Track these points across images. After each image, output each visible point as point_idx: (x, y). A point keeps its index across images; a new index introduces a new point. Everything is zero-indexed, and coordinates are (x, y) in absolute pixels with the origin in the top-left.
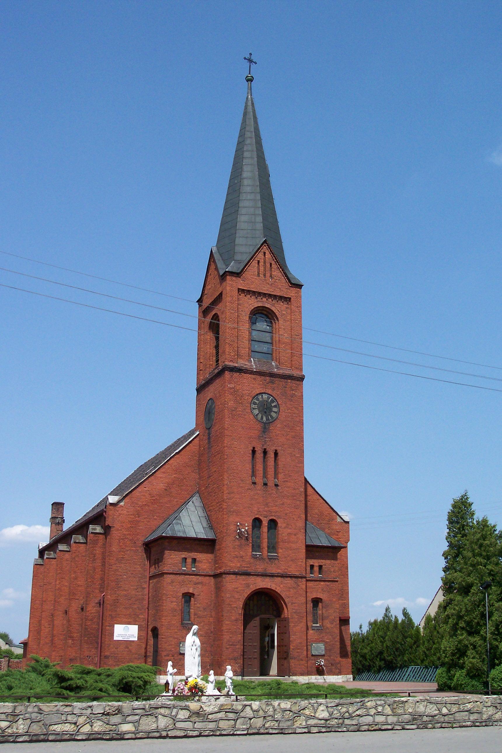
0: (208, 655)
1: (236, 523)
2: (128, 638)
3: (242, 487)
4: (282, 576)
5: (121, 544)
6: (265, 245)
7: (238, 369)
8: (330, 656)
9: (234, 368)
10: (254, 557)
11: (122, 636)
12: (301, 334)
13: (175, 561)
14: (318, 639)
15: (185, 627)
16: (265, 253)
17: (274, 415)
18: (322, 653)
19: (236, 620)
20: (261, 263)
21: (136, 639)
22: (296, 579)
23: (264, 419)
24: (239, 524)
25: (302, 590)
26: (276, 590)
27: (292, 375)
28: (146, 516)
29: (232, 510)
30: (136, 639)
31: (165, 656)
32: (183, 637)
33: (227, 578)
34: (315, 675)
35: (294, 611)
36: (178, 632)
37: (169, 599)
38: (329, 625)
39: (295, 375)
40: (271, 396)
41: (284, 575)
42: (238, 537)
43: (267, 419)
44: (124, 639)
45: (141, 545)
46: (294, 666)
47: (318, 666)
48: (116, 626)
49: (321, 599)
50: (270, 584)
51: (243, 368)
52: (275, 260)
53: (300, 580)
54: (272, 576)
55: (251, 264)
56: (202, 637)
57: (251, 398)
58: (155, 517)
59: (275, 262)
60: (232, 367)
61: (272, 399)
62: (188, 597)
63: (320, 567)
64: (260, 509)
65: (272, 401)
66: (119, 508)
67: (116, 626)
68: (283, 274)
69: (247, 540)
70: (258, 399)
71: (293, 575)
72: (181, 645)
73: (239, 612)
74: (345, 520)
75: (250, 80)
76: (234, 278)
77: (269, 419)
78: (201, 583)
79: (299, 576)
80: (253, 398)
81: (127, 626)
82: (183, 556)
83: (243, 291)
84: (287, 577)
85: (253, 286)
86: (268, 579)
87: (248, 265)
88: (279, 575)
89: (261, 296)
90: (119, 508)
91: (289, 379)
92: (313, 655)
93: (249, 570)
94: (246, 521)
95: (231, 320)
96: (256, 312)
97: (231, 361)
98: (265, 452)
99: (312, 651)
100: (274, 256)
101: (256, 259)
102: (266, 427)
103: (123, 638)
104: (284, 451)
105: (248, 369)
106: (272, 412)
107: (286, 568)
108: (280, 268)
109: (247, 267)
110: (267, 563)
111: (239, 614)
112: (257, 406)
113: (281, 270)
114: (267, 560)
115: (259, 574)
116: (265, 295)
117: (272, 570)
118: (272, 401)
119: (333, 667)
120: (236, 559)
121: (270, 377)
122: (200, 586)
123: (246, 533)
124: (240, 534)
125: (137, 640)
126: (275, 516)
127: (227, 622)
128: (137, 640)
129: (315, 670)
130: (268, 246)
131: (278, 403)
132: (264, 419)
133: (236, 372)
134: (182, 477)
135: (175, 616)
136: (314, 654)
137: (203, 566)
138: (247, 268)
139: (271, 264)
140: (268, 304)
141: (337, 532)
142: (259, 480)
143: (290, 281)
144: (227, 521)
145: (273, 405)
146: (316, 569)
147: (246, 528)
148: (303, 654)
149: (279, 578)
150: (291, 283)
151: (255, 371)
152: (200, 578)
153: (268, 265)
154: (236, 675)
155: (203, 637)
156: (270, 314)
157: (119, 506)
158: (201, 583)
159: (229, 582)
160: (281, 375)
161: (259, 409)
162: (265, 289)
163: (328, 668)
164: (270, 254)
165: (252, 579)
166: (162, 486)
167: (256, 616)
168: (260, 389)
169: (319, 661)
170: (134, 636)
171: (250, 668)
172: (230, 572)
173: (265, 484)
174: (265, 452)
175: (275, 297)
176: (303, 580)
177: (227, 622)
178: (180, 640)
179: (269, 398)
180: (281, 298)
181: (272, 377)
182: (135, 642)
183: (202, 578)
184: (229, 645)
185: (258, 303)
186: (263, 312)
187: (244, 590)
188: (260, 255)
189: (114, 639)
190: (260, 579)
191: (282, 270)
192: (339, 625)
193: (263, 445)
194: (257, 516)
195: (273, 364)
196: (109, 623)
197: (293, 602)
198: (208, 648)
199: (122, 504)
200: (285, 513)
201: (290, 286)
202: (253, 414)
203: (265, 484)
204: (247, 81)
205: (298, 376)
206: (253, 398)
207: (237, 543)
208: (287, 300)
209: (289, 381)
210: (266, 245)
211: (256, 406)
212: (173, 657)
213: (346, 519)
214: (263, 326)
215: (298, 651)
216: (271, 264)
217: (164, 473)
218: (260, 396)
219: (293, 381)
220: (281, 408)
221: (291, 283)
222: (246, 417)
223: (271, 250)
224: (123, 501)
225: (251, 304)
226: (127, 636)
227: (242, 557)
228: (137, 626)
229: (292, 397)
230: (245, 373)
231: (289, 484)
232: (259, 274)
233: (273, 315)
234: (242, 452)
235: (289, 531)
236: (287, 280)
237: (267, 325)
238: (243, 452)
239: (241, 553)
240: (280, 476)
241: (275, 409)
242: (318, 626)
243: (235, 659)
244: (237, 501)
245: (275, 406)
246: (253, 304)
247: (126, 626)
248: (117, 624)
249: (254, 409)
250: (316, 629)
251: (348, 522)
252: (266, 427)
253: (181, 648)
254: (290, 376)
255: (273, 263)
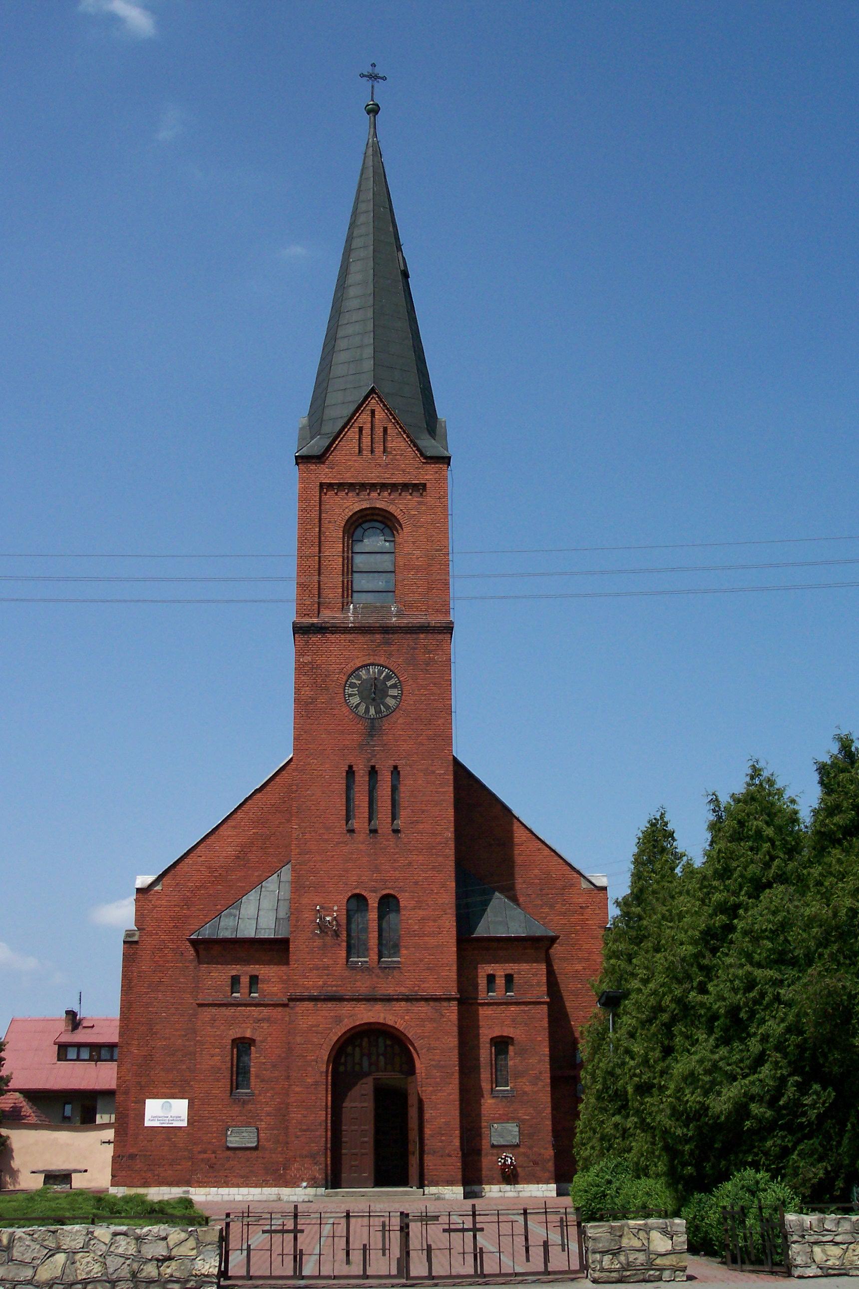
0: (280, 1149)
1: (313, 908)
2: (170, 1122)
3: (326, 840)
4: (408, 999)
5: (157, 959)
6: (373, 397)
7: (318, 627)
8: (530, 1148)
9: (311, 627)
10: (352, 967)
11: (159, 1119)
12: (446, 547)
13: (218, 983)
14: (504, 1115)
15: (237, 1100)
16: (373, 412)
17: (391, 702)
18: (514, 1141)
19: (316, 1084)
20: (367, 431)
21: (185, 1124)
22: (437, 1004)
23: (372, 711)
24: (318, 908)
25: (449, 1023)
26: (396, 1026)
27: (427, 625)
28: (202, 907)
29: (306, 883)
30: (185, 1124)
31: (200, 1152)
32: (234, 1118)
33: (298, 1008)
34: (499, 1183)
35: (433, 1063)
36: (223, 1109)
37: (206, 1050)
38: (528, 1088)
39: (433, 623)
40: (383, 667)
41: (410, 997)
42: (319, 932)
43: (378, 711)
44: (163, 1123)
45: (192, 957)
46: (434, 1167)
47: (501, 1166)
48: (148, 1101)
49: (512, 1038)
50: (382, 1015)
51: (328, 625)
52: (393, 421)
53: (445, 1004)
54: (388, 999)
55: (345, 435)
56: (269, 1117)
57: (345, 678)
58: (217, 907)
59: (393, 423)
60: (306, 625)
61: (387, 673)
62: (243, 1045)
63: (509, 978)
64: (363, 878)
65: (388, 677)
66: (153, 895)
67: (148, 1101)
68: (409, 443)
69: (338, 936)
70: (359, 678)
71: (430, 996)
72: (229, 1133)
73: (322, 1070)
74: (598, 884)
75: (374, 110)
76: (313, 467)
77: (381, 712)
78: (267, 1020)
79: (442, 997)
80: (350, 676)
81: (168, 1102)
82: (234, 973)
83: (330, 486)
84: (417, 1000)
85: (348, 475)
86: (379, 1006)
87: (339, 439)
88: (401, 997)
89: (354, 490)
90: (153, 895)
91: (422, 633)
92: (493, 1146)
93: (342, 992)
94: (335, 903)
95: (306, 541)
96: (361, 521)
97: (305, 614)
98: (373, 772)
99: (492, 1139)
100: (391, 414)
101: (356, 425)
102: (373, 728)
103: (162, 1122)
104: (411, 766)
105: (338, 625)
106: (388, 698)
107: (416, 983)
108: (402, 433)
109: (337, 443)
110: (378, 976)
111: (322, 1072)
112: (357, 689)
113: (405, 436)
114: (378, 971)
115: (360, 997)
116: (373, 487)
117: (387, 989)
118: (388, 677)
119: (538, 1168)
120: (315, 971)
121: (383, 633)
122: (265, 1025)
123: (335, 923)
124: (322, 927)
125: (186, 1125)
126: (393, 888)
127: (297, 1089)
128: (186, 1125)
129: (498, 1174)
130: (379, 397)
131: (399, 680)
132: (372, 711)
133: (315, 633)
134: (268, 833)
135: (218, 1081)
136: (495, 1143)
137: (270, 988)
138: (337, 445)
139: (385, 430)
140: (379, 500)
141: (581, 907)
142: (360, 823)
143: (422, 454)
144: (297, 905)
145: (389, 684)
146: (500, 982)
147: (335, 912)
148: (452, 1144)
149: (403, 1003)
150: (426, 458)
151: (351, 627)
152: (265, 1011)
153: (379, 432)
154: (315, 1185)
155: (272, 1117)
156: (388, 518)
157: (152, 892)
158: (267, 1020)
159: (301, 1014)
160: (404, 627)
161: (360, 693)
162: (373, 477)
163: (526, 1169)
164: (384, 411)
165: (346, 1008)
166: (231, 851)
167: (367, 1074)
168: (364, 658)
169: (503, 1157)
170: (181, 1118)
171: (355, 1172)
172: (301, 997)
173: (374, 831)
174: (373, 772)
175: (394, 487)
176: (451, 1005)
177: (297, 1089)
178: (229, 1123)
179: (380, 673)
180: (405, 486)
181: (388, 633)
182: (183, 1129)
183: (269, 1011)
184: (301, 1130)
185: (362, 503)
186: (375, 518)
187: (331, 1029)
188: (364, 418)
189: (146, 1125)
190: (364, 1006)
191: (408, 437)
192: (550, 1086)
193: (369, 760)
194: (357, 891)
195: (393, 609)
196: (136, 1098)
197: (432, 1046)
198: (281, 1137)
199: (158, 888)
200: (414, 881)
201: (423, 462)
202: (348, 706)
203: (374, 831)
204: (368, 114)
205: (439, 625)
206: (350, 676)
207: (318, 942)
208: (419, 488)
209: (422, 636)
210: (374, 396)
211: (355, 691)
212: (213, 1155)
213: (601, 881)
214: (378, 542)
215: (443, 1138)
216: (385, 430)
217: (235, 827)
218: (364, 671)
219: (430, 636)
220: (405, 688)
221: (426, 458)
222: (336, 712)
223: (384, 405)
224: (161, 883)
225: (346, 508)
226: (167, 1119)
227: (327, 968)
228: (186, 1101)
229: (427, 665)
230: (333, 634)
231: (421, 826)
232: (360, 451)
233: (393, 519)
234: (326, 777)
235: (421, 913)
236: (416, 452)
237: (385, 541)
238: (328, 777)
239: (324, 960)
240: (404, 814)
241: (394, 692)
242: (507, 1091)
243: (313, 1156)
244: (317, 867)
245: (394, 686)
246: (351, 507)
247: (166, 1102)
248: (150, 1098)
249: (350, 695)
250: (501, 1095)
251: (604, 889)
252: (373, 728)
253: (228, 1139)
254: (422, 627)
255: (390, 426)
